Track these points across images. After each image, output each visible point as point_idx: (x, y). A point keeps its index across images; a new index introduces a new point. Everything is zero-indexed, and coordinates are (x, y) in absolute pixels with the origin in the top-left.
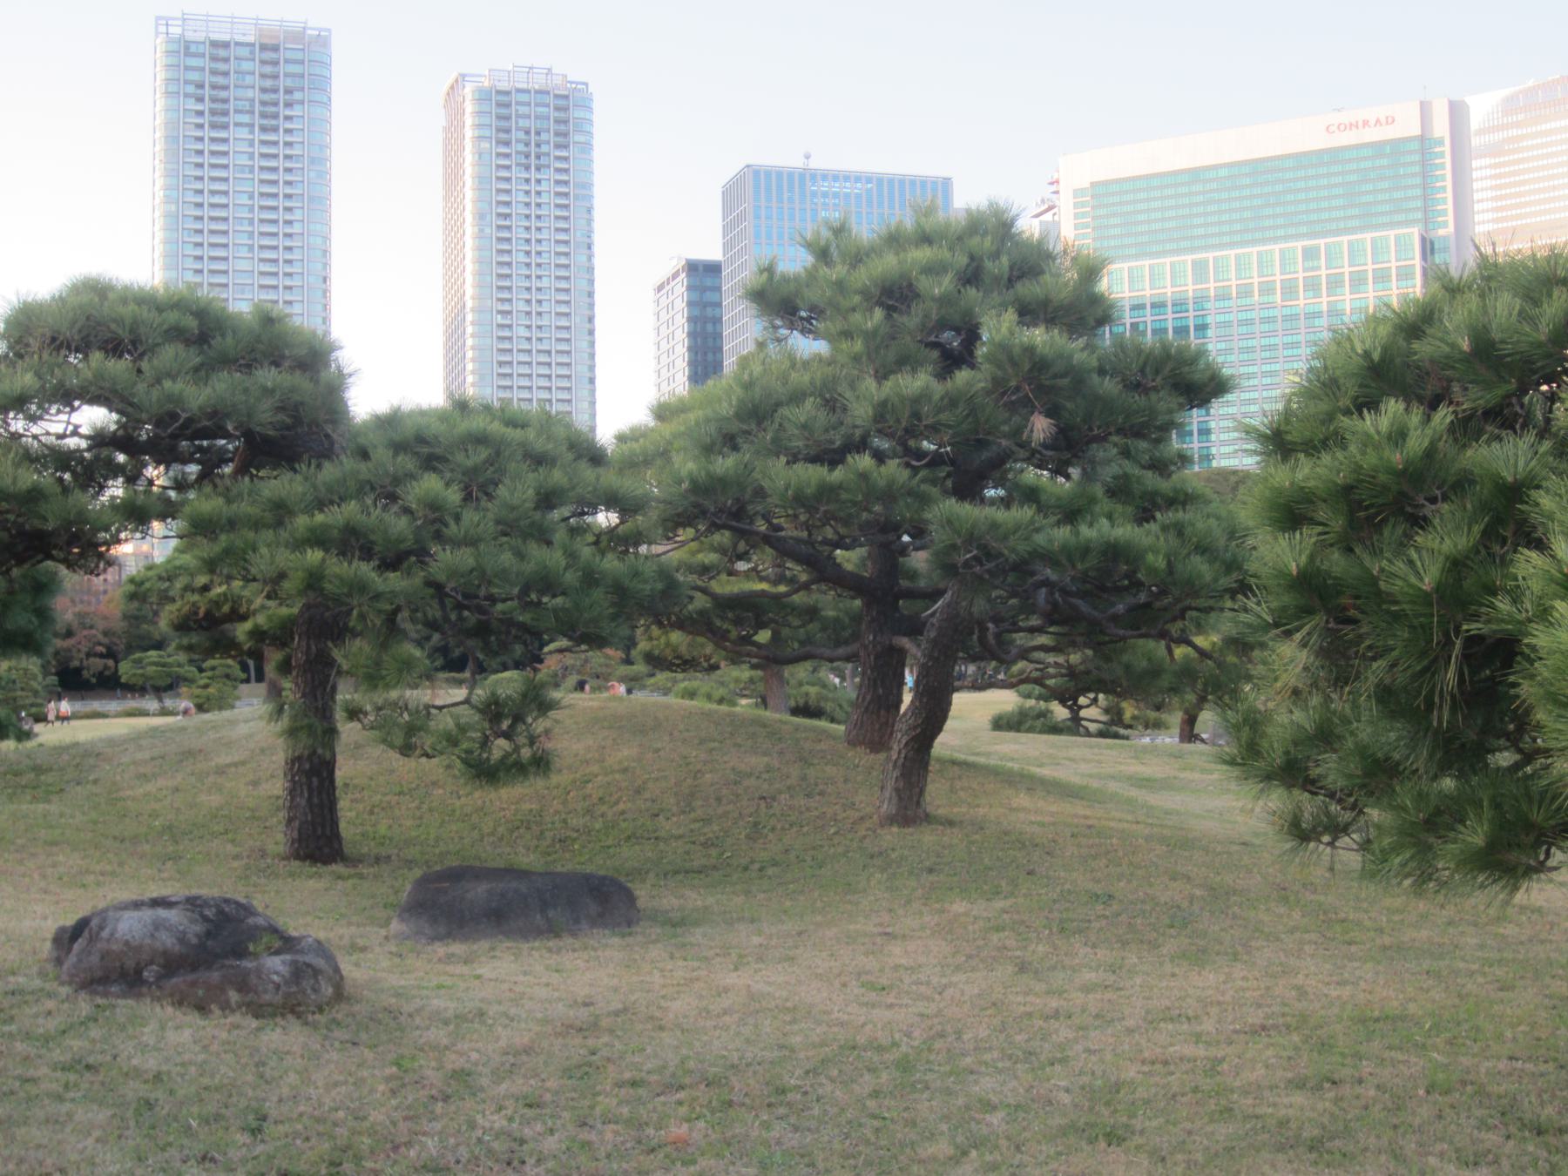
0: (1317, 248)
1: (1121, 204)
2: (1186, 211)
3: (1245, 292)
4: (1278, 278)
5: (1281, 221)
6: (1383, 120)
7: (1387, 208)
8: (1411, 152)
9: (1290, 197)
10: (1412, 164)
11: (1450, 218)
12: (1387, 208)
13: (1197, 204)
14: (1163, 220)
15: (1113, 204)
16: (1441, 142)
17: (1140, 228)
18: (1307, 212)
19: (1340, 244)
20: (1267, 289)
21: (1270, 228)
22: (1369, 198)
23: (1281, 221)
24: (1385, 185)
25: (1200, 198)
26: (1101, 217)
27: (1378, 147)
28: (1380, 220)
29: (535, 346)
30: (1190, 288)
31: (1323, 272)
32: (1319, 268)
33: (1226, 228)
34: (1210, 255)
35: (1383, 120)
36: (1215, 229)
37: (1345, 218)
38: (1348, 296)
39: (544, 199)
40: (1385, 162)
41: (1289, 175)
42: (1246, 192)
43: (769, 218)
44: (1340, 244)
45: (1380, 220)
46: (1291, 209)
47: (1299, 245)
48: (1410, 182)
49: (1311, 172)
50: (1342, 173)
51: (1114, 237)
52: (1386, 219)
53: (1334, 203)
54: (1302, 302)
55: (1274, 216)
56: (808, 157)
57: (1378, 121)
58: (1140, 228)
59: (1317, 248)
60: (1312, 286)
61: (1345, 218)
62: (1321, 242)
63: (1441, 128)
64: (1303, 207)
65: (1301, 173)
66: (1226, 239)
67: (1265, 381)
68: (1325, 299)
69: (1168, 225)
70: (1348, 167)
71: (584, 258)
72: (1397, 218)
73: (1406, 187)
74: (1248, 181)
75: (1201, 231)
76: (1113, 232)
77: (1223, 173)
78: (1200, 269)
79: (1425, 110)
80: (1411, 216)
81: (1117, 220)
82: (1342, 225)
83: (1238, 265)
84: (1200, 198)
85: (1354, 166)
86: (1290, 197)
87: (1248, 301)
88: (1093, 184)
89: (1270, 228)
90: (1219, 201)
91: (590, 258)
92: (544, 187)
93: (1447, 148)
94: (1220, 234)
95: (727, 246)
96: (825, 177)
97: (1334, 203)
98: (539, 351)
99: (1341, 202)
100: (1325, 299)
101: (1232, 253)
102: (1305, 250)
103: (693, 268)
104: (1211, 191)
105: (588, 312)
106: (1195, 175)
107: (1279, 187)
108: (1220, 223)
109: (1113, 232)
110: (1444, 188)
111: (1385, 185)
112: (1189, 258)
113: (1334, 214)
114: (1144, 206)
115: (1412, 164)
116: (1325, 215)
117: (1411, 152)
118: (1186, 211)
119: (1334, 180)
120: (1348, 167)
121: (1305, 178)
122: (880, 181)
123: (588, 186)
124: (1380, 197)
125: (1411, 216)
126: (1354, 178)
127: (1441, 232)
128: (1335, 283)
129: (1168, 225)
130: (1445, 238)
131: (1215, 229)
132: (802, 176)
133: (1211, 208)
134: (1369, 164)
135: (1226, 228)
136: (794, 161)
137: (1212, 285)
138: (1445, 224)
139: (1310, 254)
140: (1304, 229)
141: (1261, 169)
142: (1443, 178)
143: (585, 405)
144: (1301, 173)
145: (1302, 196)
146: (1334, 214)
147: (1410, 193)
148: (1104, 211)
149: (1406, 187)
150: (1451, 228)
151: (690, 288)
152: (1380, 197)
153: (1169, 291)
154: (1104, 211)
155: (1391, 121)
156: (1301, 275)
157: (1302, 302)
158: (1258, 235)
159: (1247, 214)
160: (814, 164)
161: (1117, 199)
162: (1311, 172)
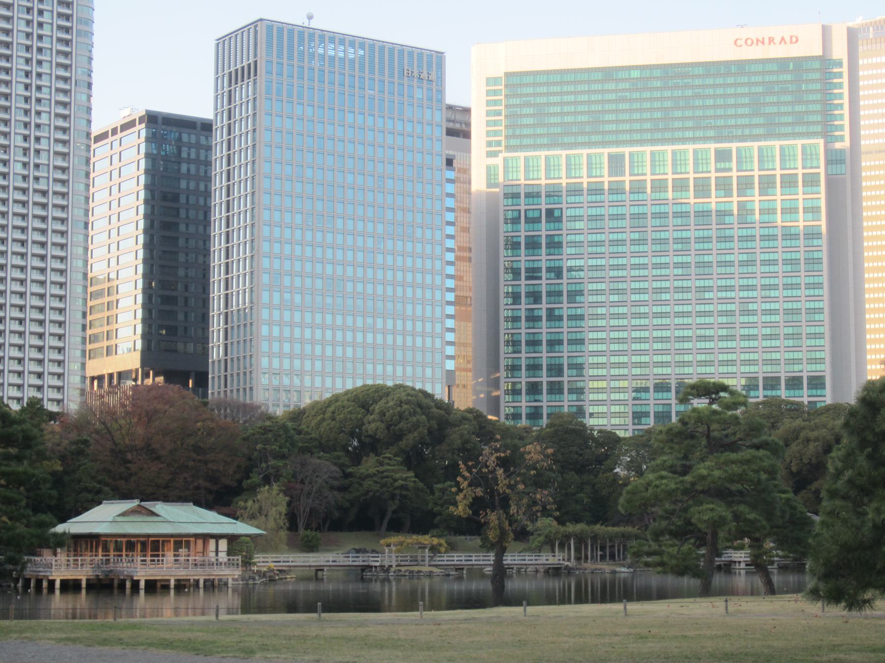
1: (534, 95)
2: (599, 107)
3: (659, 186)
4: (692, 176)
5: (690, 124)
6: (787, 39)
7: (790, 119)
8: (814, 70)
9: (698, 102)
10: (813, 81)
11: (846, 133)
12: (790, 119)
13: (609, 101)
14: (575, 113)
15: (527, 95)
16: (840, 64)
17: (553, 120)
18: (715, 117)
19: (794, 147)
20: (681, 186)
21: (679, 129)
22: (774, 109)
23: (690, 124)
24: (789, 98)
25: (612, 96)
26: (514, 106)
27: (783, 64)
28: (783, 130)
29: (32, 185)
30: (606, 179)
31: (734, 174)
32: (730, 170)
33: (637, 126)
34: (626, 150)
35: (787, 39)
36: (627, 127)
37: (750, 126)
38: (757, 198)
39: (46, 31)
40: (788, 77)
41: (697, 82)
42: (657, 94)
43: (280, 74)
44: (750, 149)
45: (783, 130)
46: (699, 113)
47: (712, 146)
48: (812, 97)
49: (720, 81)
50: (749, 84)
52: (789, 130)
53: (740, 111)
54: (713, 202)
55: (683, 119)
56: (310, 18)
57: (783, 39)
58: (553, 120)
59: (730, 151)
60: (724, 185)
61: (750, 126)
62: (734, 146)
63: (839, 51)
64: (711, 112)
65: (710, 81)
66: (637, 136)
67: (633, 273)
69: (580, 118)
70: (754, 79)
71: (84, 97)
72: (798, 129)
73: (808, 102)
74: (658, 84)
75: (613, 127)
76: (526, 121)
77: (635, 74)
78: (616, 163)
79: (826, 32)
80: (812, 128)
81: (531, 110)
82: (747, 132)
83: (653, 161)
84: (612, 96)
85: (759, 79)
86: (698, 102)
87: (662, 195)
88: (506, 74)
89: (679, 129)
90: (631, 101)
91: (89, 97)
92: (46, 18)
93: (845, 69)
94: (631, 131)
95: (226, 98)
96: (322, 38)
97: (740, 111)
98: (35, 191)
99: (746, 111)
100: (735, 199)
101: (648, 149)
102: (717, 152)
103: (152, 119)
104: (623, 90)
105: (85, 154)
106: (609, 73)
107: (689, 93)
108: (631, 121)
109: (526, 121)
110: (841, 105)
111: (789, 98)
112: (606, 151)
113: (740, 121)
114: (557, 99)
115: (813, 81)
116: (732, 122)
117: (814, 70)
118: (599, 107)
119: (740, 90)
120: (754, 79)
121: (714, 86)
122: (372, 47)
123: (89, 22)
124: (783, 109)
125: (812, 128)
126: (760, 89)
127: (838, 145)
128: (745, 184)
129: (580, 118)
130: (842, 151)
131: (627, 127)
132: (301, 34)
133: (622, 106)
134: (774, 78)
135: (637, 126)
136: (299, 19)
137: (627, 178)
138: (841, 139)
139: (722, 156)
140: (711, 133)
141: (672, 75)
142: (841, 96)
143: (80, 251)
144: (710, 81)
145: (709, 102)
146: (740, 121)
147: (812, 107)
148: (517, 101)
149: (808, 102)
150: (846, 144)
151: (148, 140)
152: (783, 109)
153: (585, 181)
154: (517, 101)
155: (794, 40)
156: (713, 175)
157: (713, 200)
158: (668, 135)
159: (658, 115)
160: (314, 24)
161: (530, 90)
162: (720, 81)
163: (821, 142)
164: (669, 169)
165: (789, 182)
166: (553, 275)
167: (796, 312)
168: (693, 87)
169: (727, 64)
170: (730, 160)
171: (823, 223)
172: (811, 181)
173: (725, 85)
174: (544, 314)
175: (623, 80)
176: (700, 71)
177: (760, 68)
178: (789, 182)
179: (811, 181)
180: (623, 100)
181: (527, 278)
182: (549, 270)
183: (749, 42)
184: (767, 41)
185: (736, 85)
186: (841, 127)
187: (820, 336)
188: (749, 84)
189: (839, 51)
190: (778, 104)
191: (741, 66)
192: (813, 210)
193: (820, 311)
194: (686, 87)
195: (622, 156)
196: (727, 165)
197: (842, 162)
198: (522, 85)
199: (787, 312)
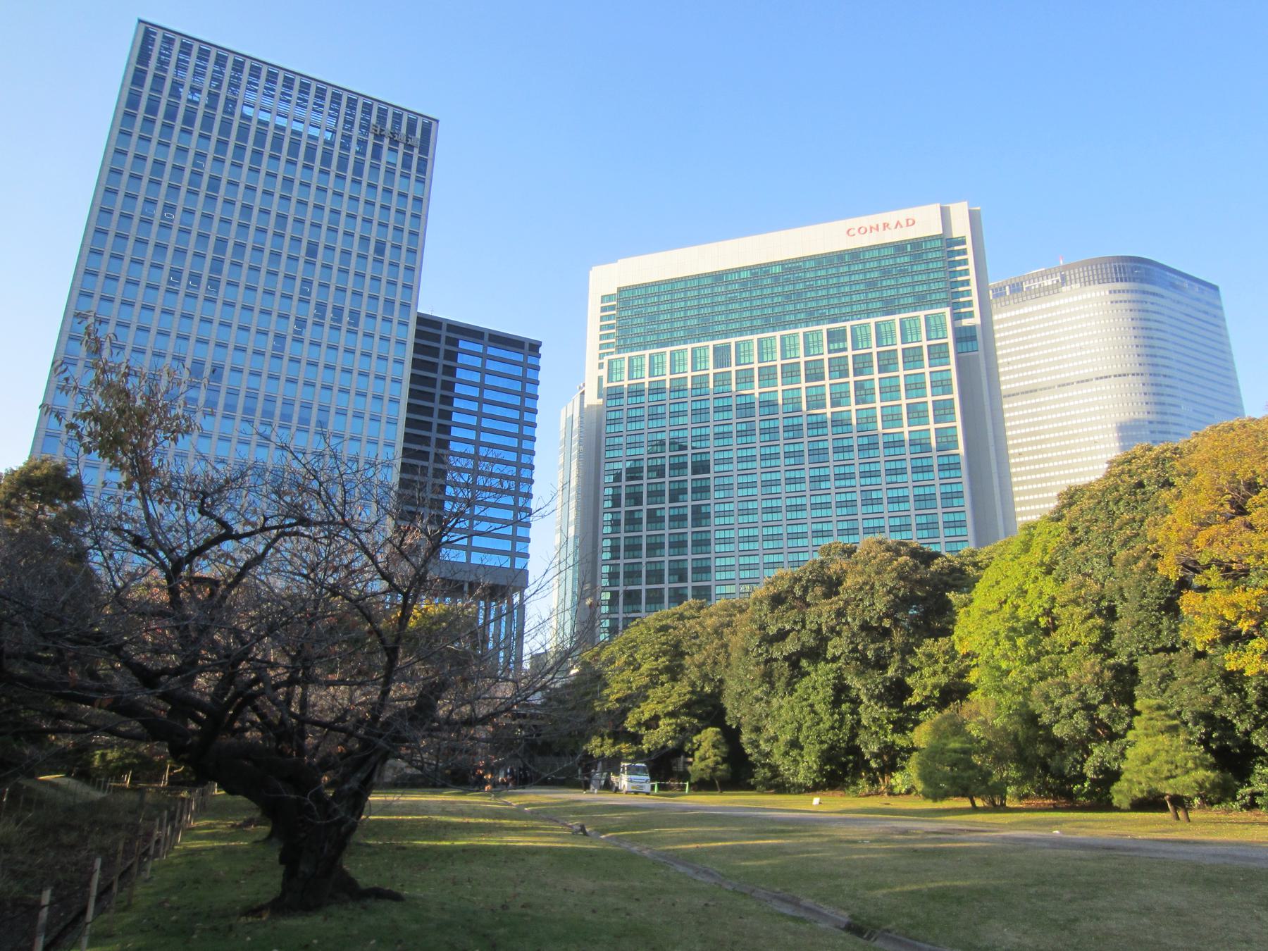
0: (843, 332)
6: (904, 223)
11: (976, 308)
27: (899, 247)
31: (850, 353)
32: (845, 349)
35: (904, 223)
47: (824, 328)
51: (638, 335)
57: (898, 223)
59: (844, 331)
63: (961, 228)
65: (823, 273)
68: (851, 379)
77: (745, 275)
78: (721, 356)
88: (620, 290)
93: (969, 246)
100: (851, 379)
104: (733, 291)
106: (718, 277)
115: (936, 260)
121: (827, 277)
127: (965, 322)
130: (972, 328)
139: (834, 336)
150: (976, 320)
155: (911, 223)
163: (947, 311)
164: (778, 355)
165: (912, 357)
166: (655, 474)
167: (931, 497)
168: (804, 280)
169: (840, 256)
170: (845, 340)
171: (955, 396)
172: (938, 353)
173: (838, 276)
174: (644, 516)
175: (733, 282)
176: (813, 264)
177: (876, 254)
178: (912, 357)
179: (938, 353)
180: (733, 300)
181: (628, 479)
182: (650, 469)
183: (862, 231)
184: (881, 227)
185: (850, 274)
186: (970, 304)
187: (962, 524)
188: (864, 272)
189: (961, 228)
190: (897, 287)
191: (855, 254)
192: (942, 385)
193: (959, 495)
194: (798, 280)
195: (728, 347)
196: (841, 346)
197: (973, 338)
198: (635, 298)
199: (918, 498)
